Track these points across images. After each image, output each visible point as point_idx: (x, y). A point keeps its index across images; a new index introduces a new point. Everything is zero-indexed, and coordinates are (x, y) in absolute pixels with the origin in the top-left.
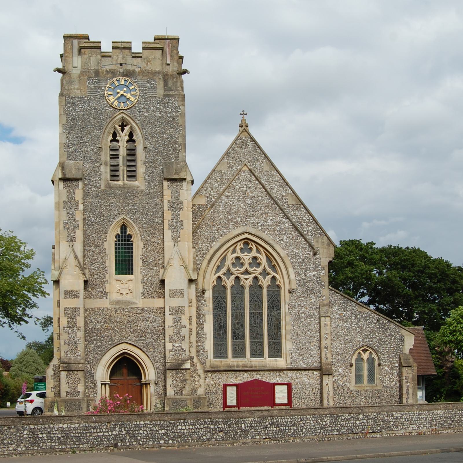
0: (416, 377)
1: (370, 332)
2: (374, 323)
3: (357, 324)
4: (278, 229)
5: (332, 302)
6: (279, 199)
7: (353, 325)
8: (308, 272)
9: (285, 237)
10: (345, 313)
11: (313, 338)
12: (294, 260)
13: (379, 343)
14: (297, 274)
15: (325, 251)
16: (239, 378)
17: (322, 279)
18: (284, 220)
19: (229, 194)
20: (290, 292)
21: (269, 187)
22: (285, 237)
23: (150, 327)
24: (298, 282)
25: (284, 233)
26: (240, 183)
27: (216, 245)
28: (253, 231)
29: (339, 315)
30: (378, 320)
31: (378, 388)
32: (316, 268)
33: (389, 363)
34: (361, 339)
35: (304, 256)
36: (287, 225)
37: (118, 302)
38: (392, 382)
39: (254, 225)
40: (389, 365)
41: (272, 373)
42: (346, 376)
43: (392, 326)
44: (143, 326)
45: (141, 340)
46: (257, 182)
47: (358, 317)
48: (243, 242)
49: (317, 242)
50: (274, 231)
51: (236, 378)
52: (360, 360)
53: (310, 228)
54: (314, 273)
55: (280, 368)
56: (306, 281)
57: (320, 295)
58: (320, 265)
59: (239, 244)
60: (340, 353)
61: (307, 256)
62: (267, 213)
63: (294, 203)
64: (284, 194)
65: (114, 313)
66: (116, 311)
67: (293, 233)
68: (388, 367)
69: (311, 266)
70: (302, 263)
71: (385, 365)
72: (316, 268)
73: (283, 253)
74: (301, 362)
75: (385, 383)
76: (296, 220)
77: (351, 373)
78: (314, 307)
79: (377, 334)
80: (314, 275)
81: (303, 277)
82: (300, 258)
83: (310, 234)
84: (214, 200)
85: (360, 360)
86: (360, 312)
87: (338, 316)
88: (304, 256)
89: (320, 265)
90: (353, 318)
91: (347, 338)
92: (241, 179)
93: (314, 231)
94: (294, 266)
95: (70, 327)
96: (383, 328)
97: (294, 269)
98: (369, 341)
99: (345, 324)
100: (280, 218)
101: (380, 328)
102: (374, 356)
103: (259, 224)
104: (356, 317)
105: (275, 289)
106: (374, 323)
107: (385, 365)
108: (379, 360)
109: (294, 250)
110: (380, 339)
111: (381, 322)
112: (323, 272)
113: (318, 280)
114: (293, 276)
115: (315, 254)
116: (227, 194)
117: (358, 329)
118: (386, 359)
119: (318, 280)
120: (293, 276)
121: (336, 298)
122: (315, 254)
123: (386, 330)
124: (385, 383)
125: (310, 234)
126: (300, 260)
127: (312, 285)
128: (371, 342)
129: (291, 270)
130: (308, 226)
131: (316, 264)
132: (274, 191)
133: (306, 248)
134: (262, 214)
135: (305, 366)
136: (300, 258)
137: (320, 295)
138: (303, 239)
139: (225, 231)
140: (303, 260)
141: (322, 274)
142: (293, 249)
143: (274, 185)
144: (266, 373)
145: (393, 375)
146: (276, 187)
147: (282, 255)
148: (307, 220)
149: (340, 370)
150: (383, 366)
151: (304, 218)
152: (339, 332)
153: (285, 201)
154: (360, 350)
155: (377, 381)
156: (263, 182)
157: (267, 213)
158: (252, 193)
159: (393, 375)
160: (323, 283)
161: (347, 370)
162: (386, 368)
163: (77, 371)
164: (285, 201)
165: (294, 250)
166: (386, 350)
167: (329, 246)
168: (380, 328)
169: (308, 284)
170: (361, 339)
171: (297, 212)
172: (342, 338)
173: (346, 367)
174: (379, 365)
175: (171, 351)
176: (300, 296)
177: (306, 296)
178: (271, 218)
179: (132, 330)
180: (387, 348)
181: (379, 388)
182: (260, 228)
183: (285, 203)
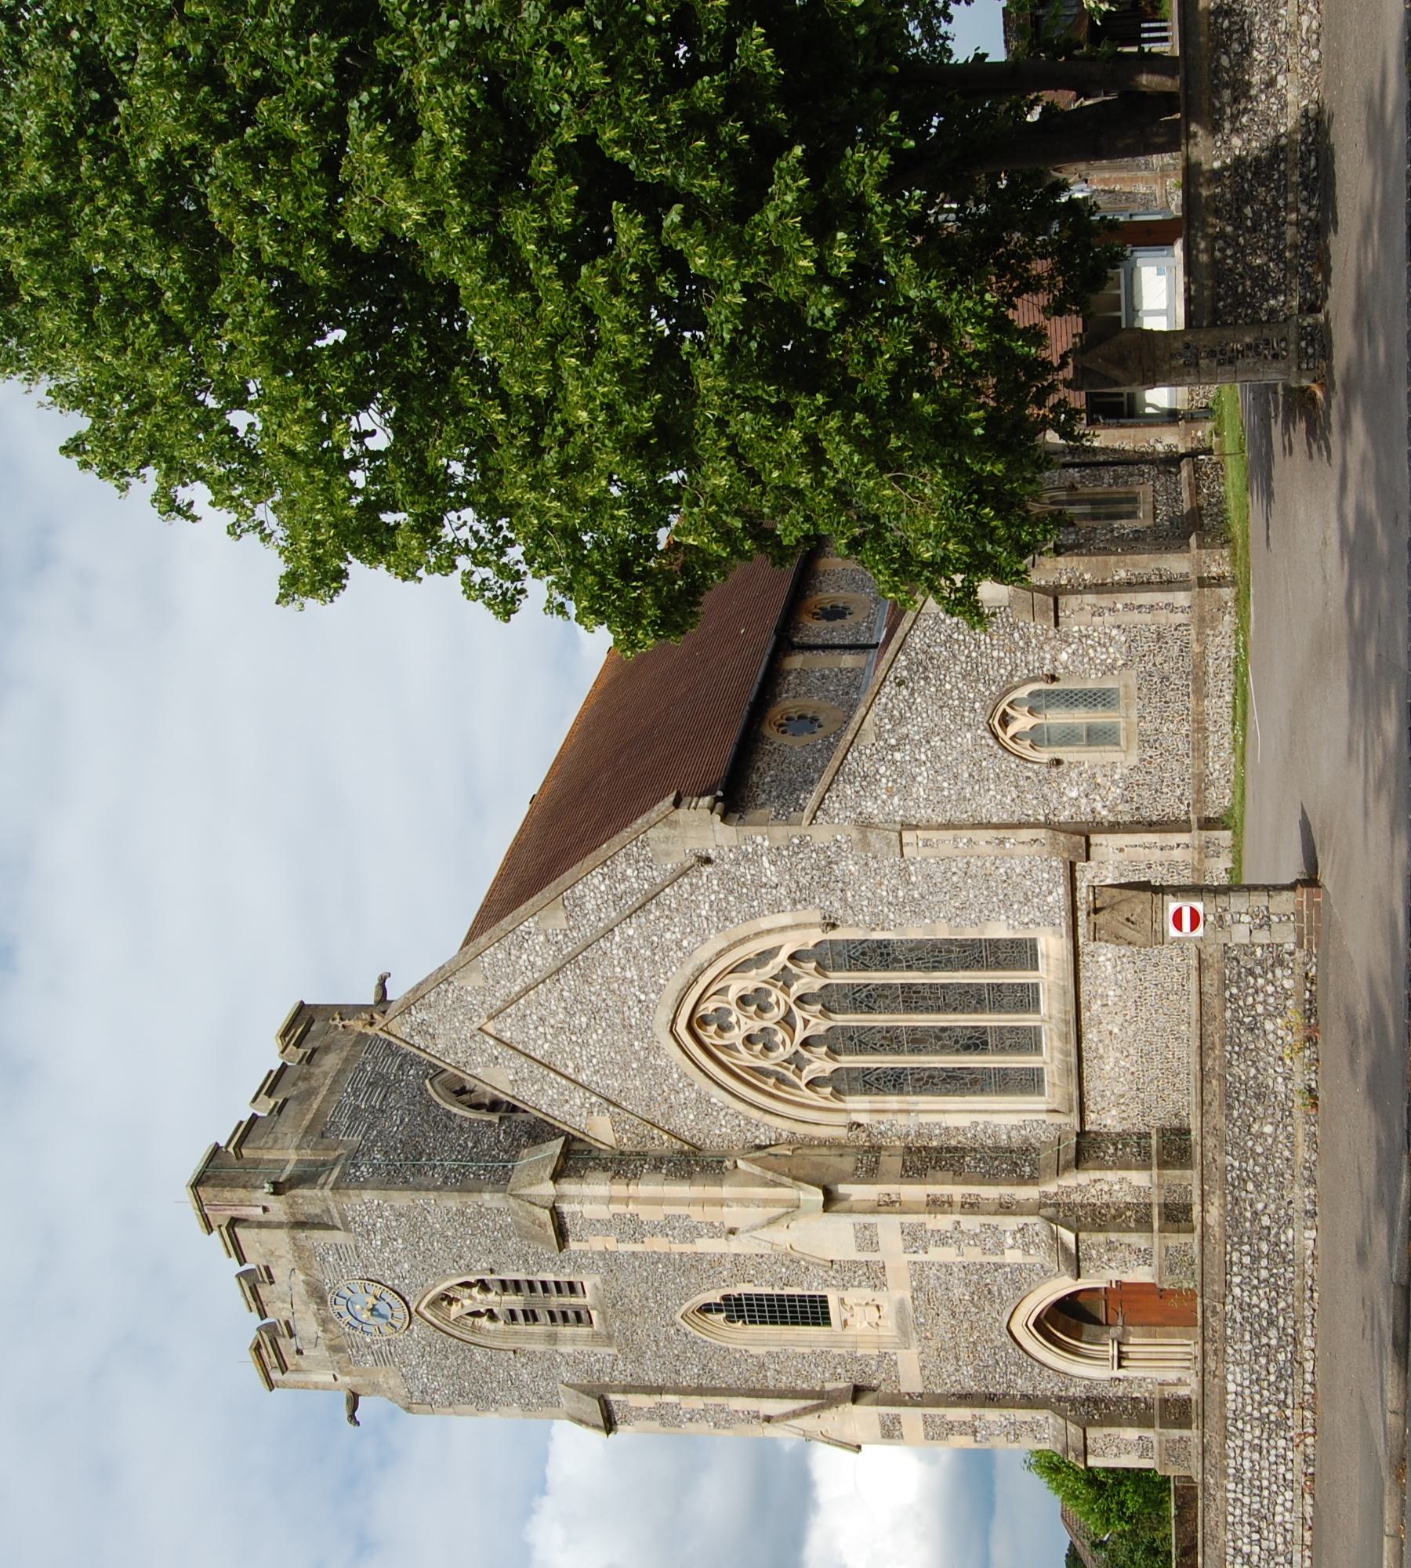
0: (1094, 559)
1: (941, 707)
2: (912, 694)
3: (919, 745)
4: (648, 953)
5: (853, 816)
6: (560, 950)
7: (923, 757)
8: (764, 880)
9: (668, 935)
10: (884, 780)
11: (973, 870)
12: (734, 914)
13: (977, 681)
14: (776, 907)
15: (691, 833)
16: (1101, 1051)
17: (783, 843)
18: (617, 939)
19: (570, 1064)
20: (834, 926)
21: (529, 974)
22: (668, 935)
23: (962, 1275)
24: (799, 906)
25: (655, 939)
26: (535, 1041)
27: (718, 1096)
28: (664, 1015)
29: (891, 796)
30: (899, 685)
31: (1133, 683)
32: (751, 859)
33: (1046, 647)
34: (969, 735)
35: (716, 888)
36: (631, 932)
37: (903, 1331)
38: (1111, 639)
39: (646, 1008)
40: (1053, 648)
41: (1084, 974)
42: (1094, 776)
43: (916, 641)
44: (962, 1289)
45: (1000, 1293)
46: (522, 1001)
47: (893, 742)
48: (700, 1032)
49: (668, 854)
50: (654, 962)
51: (1101, 1057)
52: (1038, 737)
53: (629, 872)
54: (767, 865)
55: (1071, 958)
56: (793, 885)
57: (834, 849)
58: (738, 847)
59: (707, 1040)
60: (1014, 794)
61: (715, 882)
62: (607, 981)
63: (562, 915)
64: (542, 938)
65: (931, 1343)
66: (926, 1338)
67: (652, 917)
68: (1060, 651)
69: (747, 872)
70: (741, 895)
71: (1054, 659)
72: (751, 859)
73: (716, 943)
74: (1050, 899)
75: (1115, 660)
76: (611, 909)
77: (1081, 763)
78: (873, 864)
79: (948, 686)
80: (773, 863)
81: (783, 890)
82: (726, 898)
83: (647, 873)
84: (594, 1099)
85: (1038, 737)
86: (878, 737)
87: (896, 799)
88: (716, 888)
89: (738, 847)
90: (898, 756)
91: (966, 775)
92: (521, 1037)
93: (637, 862)
94: (753, 916)
95: (975, 1432)
96: (926, 669)
97: (761, 914)
98: (973, 710)
99: (919, 779)
100: (614, 946)
101: (926, 678)
102: (1023, 692)
103: (643, 997)
104: (893, 748)
105: (825, 957)
106: (912, 694)
107: (1054, 659)
108: (1035, 679)
109: (704, 913)
110: (964, 678)
111: (905, 673)
112: (759, 839)
113: (785, 853)
114: (785, 919)
115: (708, 861)
116: (571, 1070)
117: (936, 741)
118: (1030, 658)
119: (785, 853)
120: (785, 919)
121: (837, 805)
122: (708, 861)
123: (931, 658)
124: (1115, 660)
125: (647, 873)
126: (731, 898)
127: (803, 869)
128: (977, 705)
129: (764, 923)
130: (624, 878)
131: (736, 859)
132: (539, 962)
133: (691, 884)
134: (613, 992)
135: (1061, 890)
136: (726, 898)
137: (834, 849)
138: (667, 890)
139: (676, 1076)
140: (731, 892)
141: (766, 844)
142: (699, 916)
143: (521, 962)
144: (1084, 988)
145: (1087, 637)
146: (524, 957)
147: (724, 944)
148: (607, 882)
149: (1074, 794)
150: (1055, 668)
151: (603, 888)
152: (949, 796)
153: (560, 937)
154: (1005, 737)
155: (1109, 684)
156: (517, 988)
157: (607, 981)
158: (554, 1014)
159: (1087, 637)
160: (796, 841)
161: (1074, 775)
162: (1064, 656)
163: (1085, 1438)
164: (560, 937)
165: (704, 913)
166: (999, 659)
167: (676, 822)
168: (926, 678)
169: (803, 881)
170: (969, 735)
171: (589, 906)
172: (968, 790)
173: (1062, 776)
174: (1054, 678)
175: (1026, 1252)
176: (843, 899)
177: (840, 885)
178: (618, 970)
179: (973, 1309)
180: (995, 654)
181: (1131, 678)
182: (653, 996)
183: (566, 935)
